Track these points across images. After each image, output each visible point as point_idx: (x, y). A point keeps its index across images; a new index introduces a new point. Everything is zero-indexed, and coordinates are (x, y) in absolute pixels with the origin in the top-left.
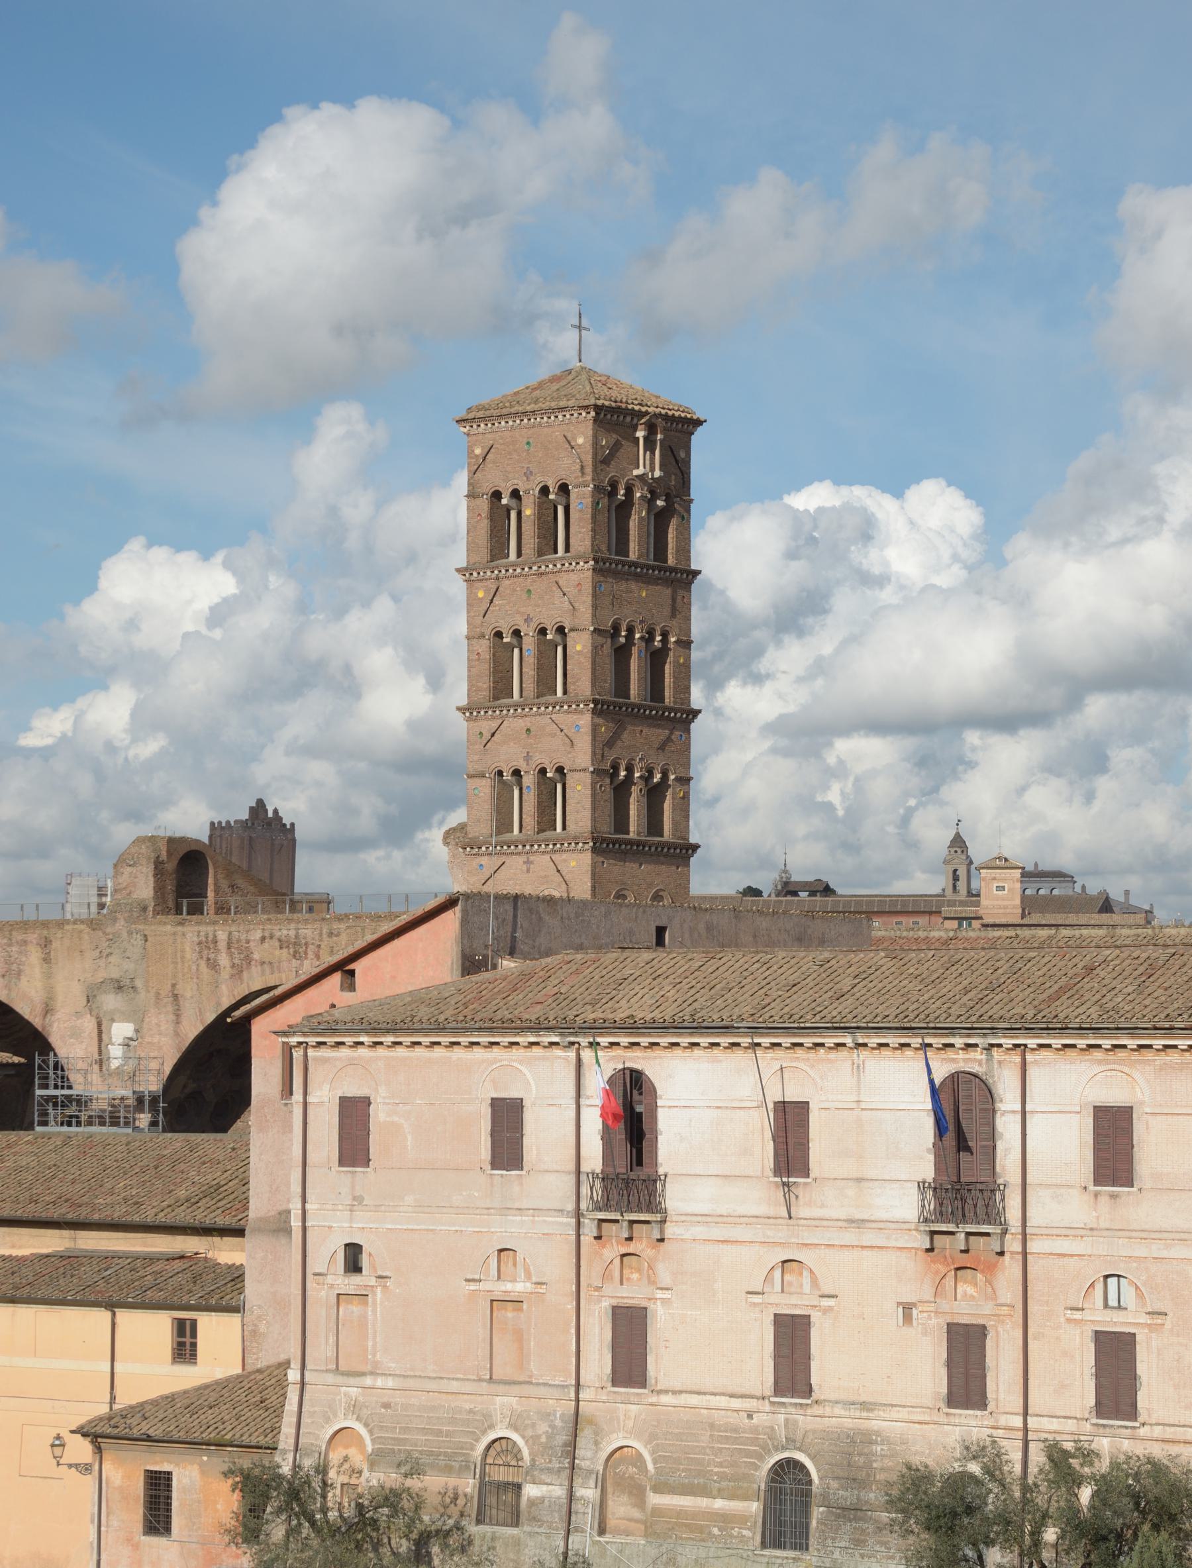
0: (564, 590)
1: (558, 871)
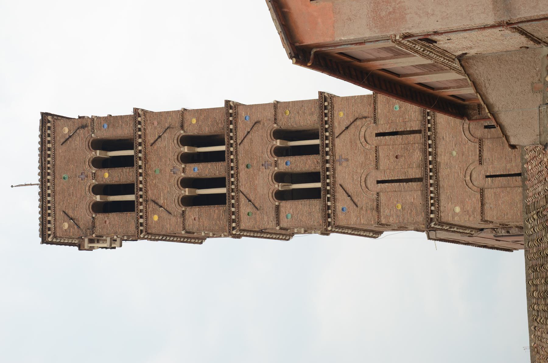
1: (347, 128)
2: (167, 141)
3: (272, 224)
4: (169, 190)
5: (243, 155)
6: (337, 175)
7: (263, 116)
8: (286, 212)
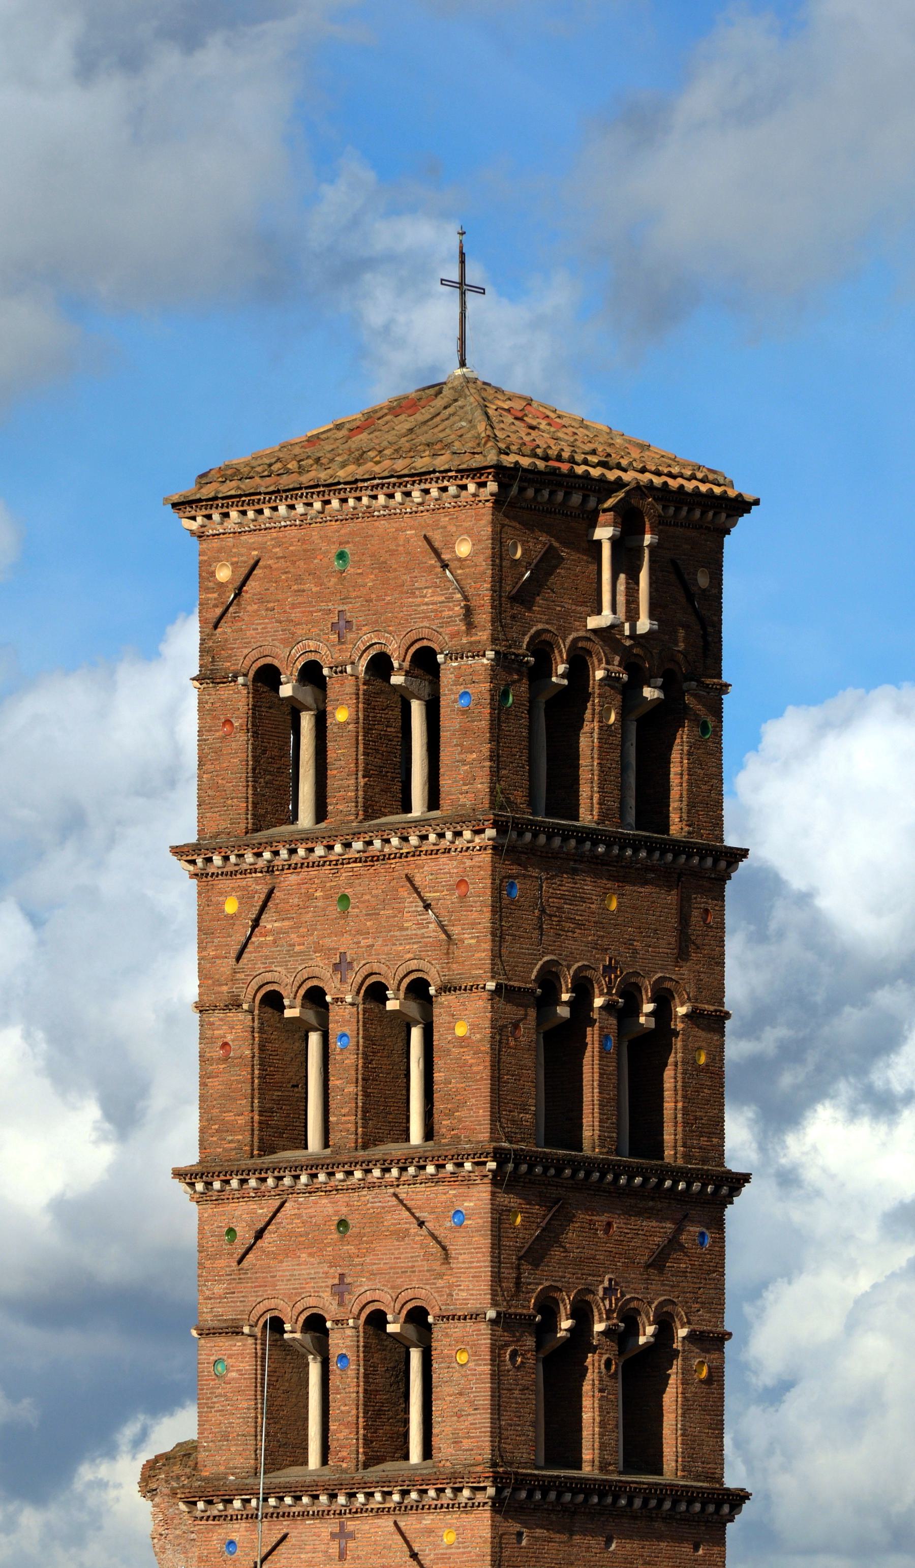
0: (428, 895)
1: (414, 1556)
2: (416, 935)
3: (205, 1310)
4: (297, 948)
5: (370, 1205)
6: (310, 1524)
7: (461, 1273)
8: (230, 1356)
